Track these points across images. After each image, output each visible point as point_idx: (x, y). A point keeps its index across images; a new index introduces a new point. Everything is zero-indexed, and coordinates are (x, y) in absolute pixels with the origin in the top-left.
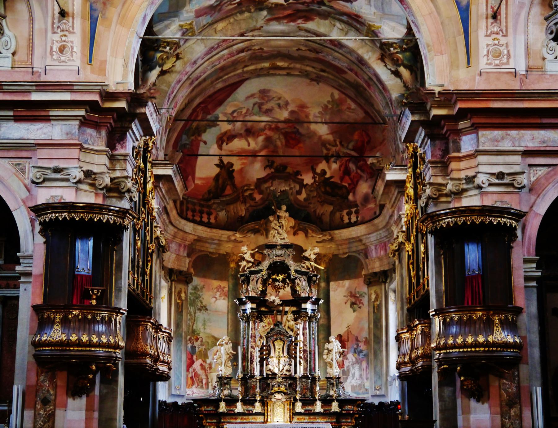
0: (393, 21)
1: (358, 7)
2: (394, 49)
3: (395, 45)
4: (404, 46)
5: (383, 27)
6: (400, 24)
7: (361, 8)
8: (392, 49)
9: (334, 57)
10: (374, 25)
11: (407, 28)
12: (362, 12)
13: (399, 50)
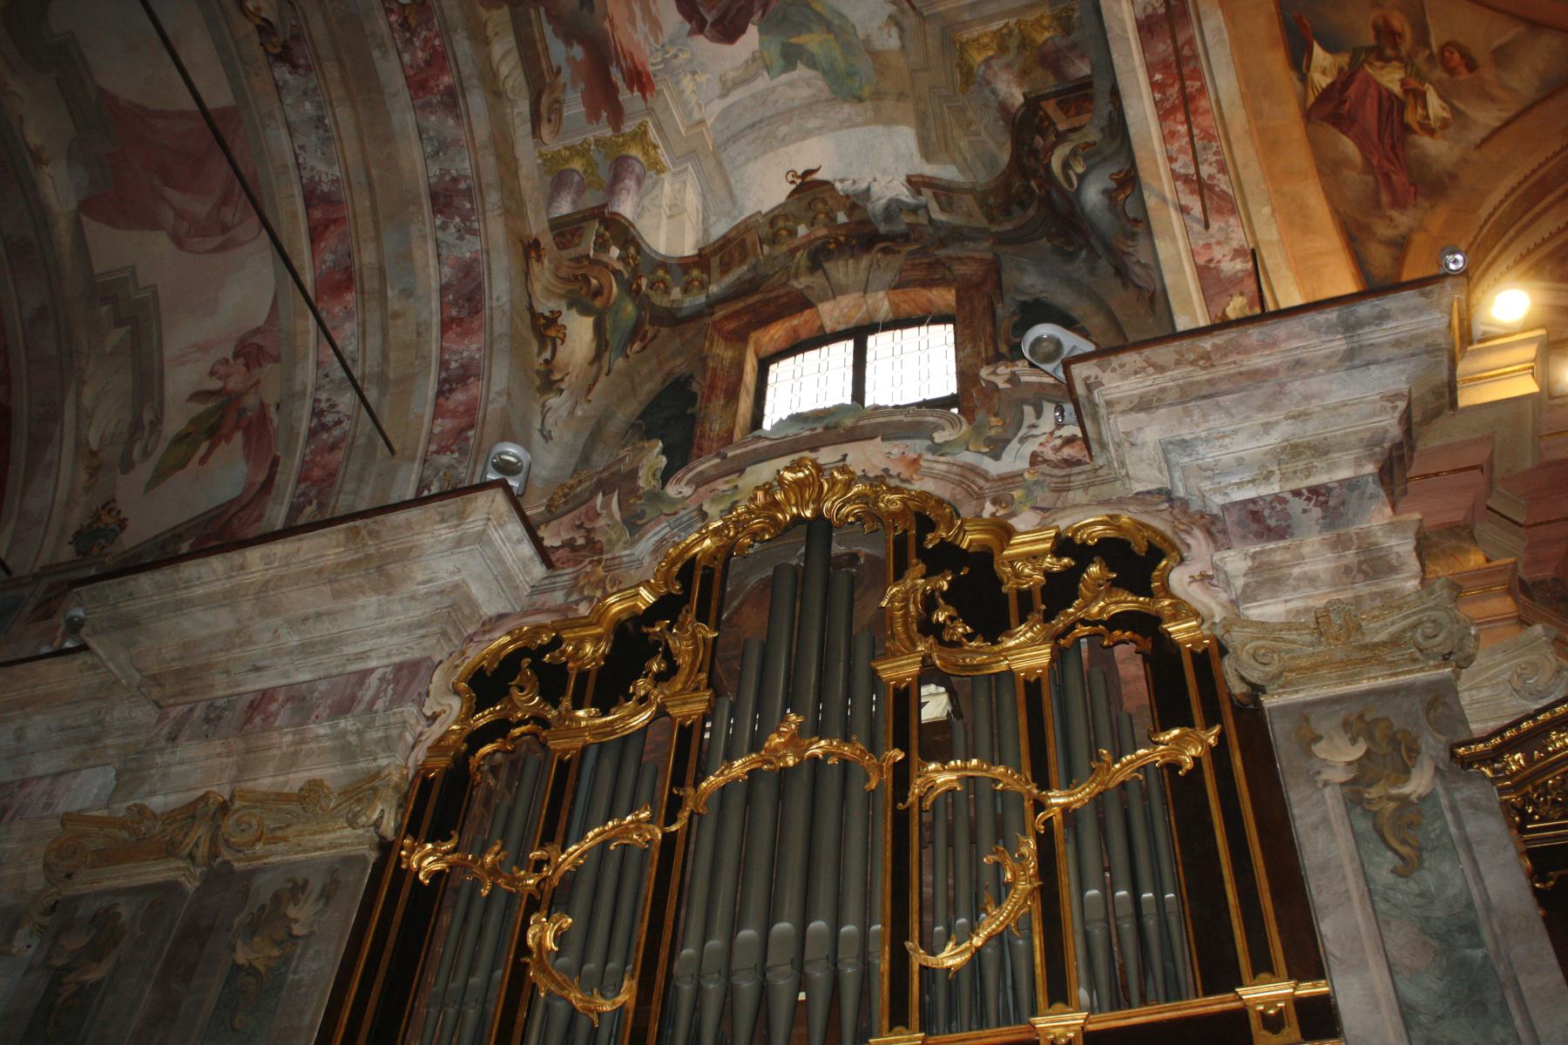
0: (704, 196)
1: (690, 61)
2: (620, 258)
3: (632, 251)
4: (644, 282)
5: (666, 177)
6: (705, 220)
7: (694, 73)
8: (615, 252)
9: (321, 119)
10: (656, 147)
11: (701, 250)
12: (678, 83)
13: (626, 275)
